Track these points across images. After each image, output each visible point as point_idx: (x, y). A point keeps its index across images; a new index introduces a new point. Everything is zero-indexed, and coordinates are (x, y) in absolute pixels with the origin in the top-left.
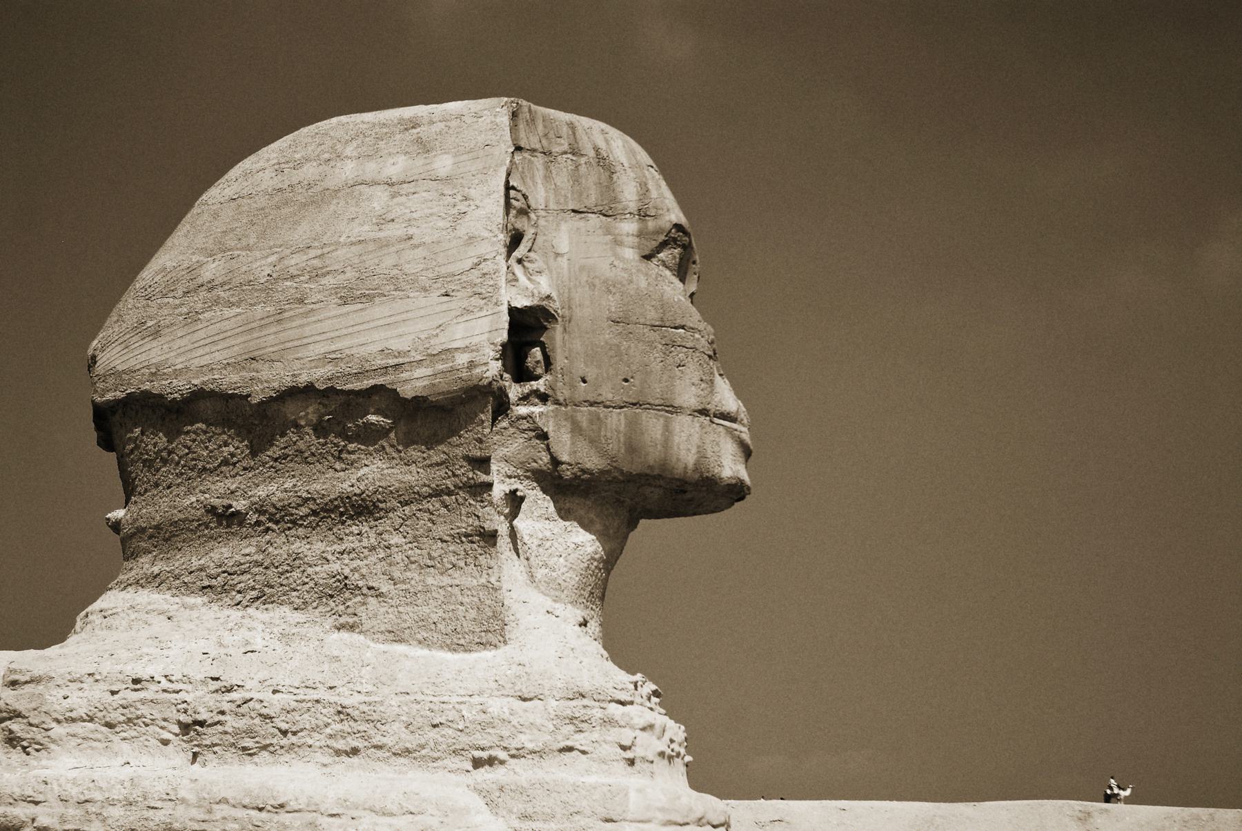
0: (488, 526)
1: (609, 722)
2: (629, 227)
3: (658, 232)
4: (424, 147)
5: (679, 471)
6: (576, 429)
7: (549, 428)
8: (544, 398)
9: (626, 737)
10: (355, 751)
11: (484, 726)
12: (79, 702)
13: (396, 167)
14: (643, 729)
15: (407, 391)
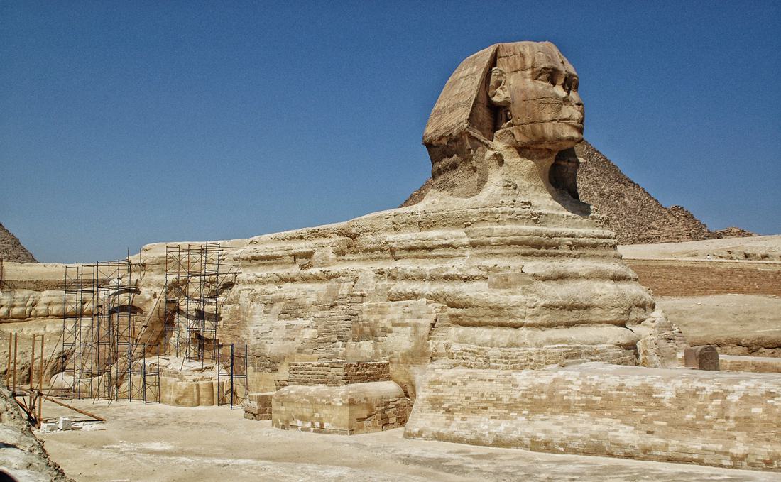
0: (474, 165)
1: (492, 213)
2: (529, 72)
3: (537, 72)
4: (474, 65)
5: (549, 139)
6: (520, 132)
7: (514, 132)
8: (511, 125)
9: (496, 216)
10: (445, 226)
11: (467, 216)
12: (404, 218)
13: (467, 72)
14: (502, 213)
15: (454, 134)
